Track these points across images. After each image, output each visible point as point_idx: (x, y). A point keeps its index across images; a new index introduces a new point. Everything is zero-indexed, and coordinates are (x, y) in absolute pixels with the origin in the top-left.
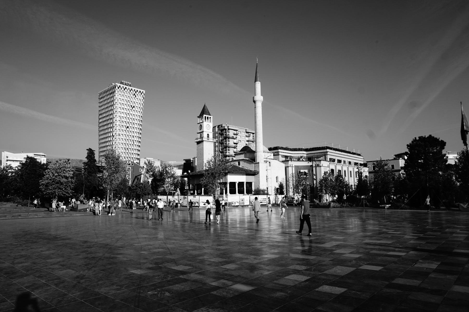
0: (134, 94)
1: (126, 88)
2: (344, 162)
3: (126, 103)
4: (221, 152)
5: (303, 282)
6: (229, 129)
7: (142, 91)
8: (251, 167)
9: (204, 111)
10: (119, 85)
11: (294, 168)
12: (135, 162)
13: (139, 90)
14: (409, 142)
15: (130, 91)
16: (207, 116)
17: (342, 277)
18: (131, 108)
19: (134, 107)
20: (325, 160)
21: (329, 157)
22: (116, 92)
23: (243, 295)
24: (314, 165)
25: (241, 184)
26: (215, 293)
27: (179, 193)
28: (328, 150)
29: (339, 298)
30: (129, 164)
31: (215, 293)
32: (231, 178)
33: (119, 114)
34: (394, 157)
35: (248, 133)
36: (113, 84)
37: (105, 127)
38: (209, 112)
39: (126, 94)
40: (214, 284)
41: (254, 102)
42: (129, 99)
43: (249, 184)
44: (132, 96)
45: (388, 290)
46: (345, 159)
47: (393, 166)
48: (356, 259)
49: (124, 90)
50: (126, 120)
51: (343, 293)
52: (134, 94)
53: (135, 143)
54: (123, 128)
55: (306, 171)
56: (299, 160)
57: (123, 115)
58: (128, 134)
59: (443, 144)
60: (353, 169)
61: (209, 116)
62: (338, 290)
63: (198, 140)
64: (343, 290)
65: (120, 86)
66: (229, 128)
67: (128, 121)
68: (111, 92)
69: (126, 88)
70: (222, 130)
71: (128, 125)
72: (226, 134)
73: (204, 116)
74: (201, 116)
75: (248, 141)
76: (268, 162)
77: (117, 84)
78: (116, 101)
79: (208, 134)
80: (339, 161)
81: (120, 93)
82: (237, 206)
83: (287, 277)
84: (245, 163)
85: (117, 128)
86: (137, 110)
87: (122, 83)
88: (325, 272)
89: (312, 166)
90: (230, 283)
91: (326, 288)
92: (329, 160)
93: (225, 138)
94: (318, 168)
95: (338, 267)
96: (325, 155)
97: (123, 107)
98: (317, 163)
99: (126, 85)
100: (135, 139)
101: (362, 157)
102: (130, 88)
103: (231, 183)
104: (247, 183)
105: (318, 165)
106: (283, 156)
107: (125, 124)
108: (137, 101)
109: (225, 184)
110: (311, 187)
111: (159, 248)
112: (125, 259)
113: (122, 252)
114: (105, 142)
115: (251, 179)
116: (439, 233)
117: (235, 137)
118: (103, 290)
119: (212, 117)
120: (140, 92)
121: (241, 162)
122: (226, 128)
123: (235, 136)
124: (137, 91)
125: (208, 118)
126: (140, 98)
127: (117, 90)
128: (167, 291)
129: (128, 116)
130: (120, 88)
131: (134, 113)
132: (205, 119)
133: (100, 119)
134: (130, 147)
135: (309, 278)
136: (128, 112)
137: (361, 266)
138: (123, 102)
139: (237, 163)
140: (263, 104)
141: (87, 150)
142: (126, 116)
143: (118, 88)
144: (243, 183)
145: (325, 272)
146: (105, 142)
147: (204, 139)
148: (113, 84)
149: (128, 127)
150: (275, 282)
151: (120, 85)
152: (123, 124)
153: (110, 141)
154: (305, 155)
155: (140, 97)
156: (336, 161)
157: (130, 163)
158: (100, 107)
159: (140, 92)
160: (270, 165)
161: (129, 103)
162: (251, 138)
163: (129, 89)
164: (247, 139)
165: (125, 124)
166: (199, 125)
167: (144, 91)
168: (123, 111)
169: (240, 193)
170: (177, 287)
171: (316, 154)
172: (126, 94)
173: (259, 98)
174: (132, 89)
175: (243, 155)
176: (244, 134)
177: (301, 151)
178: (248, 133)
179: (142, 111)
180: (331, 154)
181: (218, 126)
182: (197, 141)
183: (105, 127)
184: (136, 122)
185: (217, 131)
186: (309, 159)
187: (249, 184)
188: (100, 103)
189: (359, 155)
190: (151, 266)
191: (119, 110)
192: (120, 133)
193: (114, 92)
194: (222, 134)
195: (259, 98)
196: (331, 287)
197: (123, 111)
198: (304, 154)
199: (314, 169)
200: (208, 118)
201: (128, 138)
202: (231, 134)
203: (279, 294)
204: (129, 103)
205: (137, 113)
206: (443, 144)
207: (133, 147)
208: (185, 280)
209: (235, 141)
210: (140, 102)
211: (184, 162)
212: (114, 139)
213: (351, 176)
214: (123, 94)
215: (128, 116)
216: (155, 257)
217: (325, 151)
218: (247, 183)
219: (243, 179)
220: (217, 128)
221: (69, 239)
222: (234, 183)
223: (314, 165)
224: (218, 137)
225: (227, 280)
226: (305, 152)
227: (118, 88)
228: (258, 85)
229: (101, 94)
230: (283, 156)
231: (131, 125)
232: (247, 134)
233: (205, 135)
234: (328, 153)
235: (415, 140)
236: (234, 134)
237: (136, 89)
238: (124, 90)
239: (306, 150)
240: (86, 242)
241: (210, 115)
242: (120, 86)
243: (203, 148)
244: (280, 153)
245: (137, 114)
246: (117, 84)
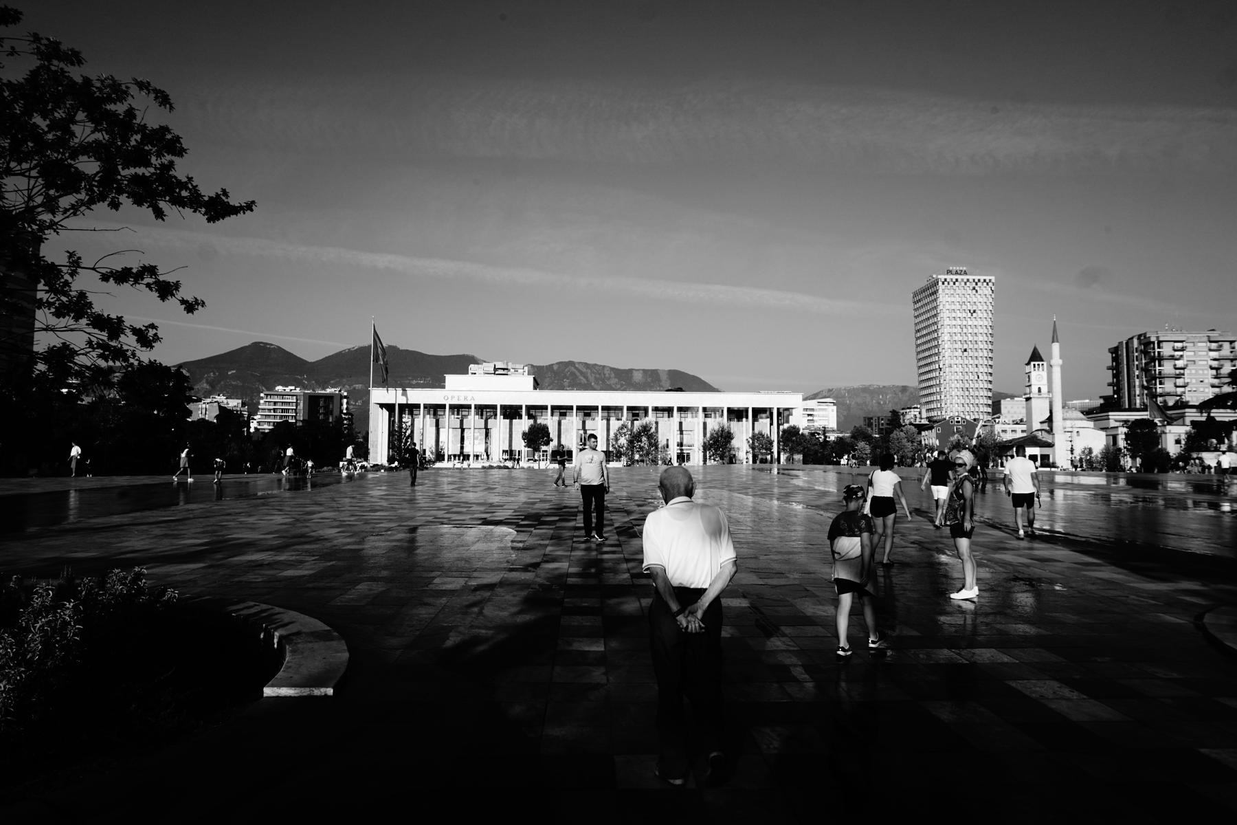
10: (942, 277)
13: (982, 278)
26: (1175, 675)
33: (946, 330)
37: (927, 354)
68: (929, 292)
85: (947, 355)
87: (949, 272)
93: (1153, 360)
99: (957, 273)
102: (965, 277)
122: (1153, 339)
123: (1178, 354)
133: (917, 339)
155: (985, 290)
164: (1214, 354)
167: (993, 278)
176: (1204, 345)
183: (927, 354)
193: (936, 292)
194: (1145, 353)
202: (1167, 350)
205: (982, 322)
209: (1180, 363)
211: (1102, 401)
229: (915, 295)
232: (1214, 346)
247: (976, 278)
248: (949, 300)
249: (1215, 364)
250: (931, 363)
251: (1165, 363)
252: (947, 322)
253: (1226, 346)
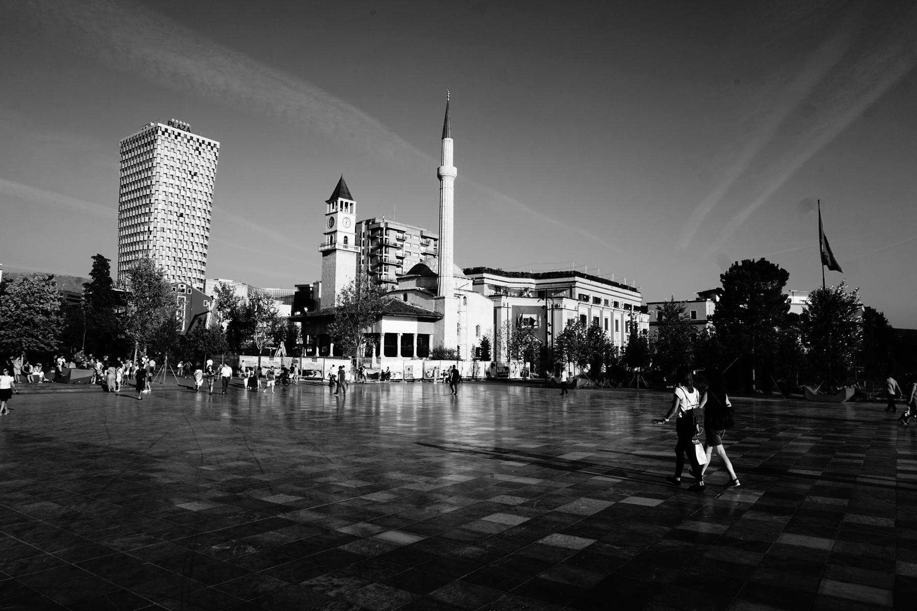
0: (197, 149)
1: (179, 134)
2: (606, 302)
3: (179, 165)
4: (371, 274)
5: (515, 527)
6: (387, 229)
7: (213, 142)
8: (428, 305)
9: (340, 191)
10: (164, 127)
11: (510, 310)
12: (195, 286)
13: (207, 140)
14: (725, 270)
15: (189, 141)
16: (345, 201)
17: (589, 519)
18: (190, 177)
19: (195, 174)
20: (571, 297)
21: (577, 292)
22: (159, 142)
23: (401, 550)
24: (549, 306)
25: (407, 338)
26: (346, 547)
27: (284, 353)
28: (577, 278)
29: (580, 558)
30: (183, 291)
31: (346, 547)
32: (388, 326)
33: (163, 188)
34: (698, 296)
35: (425, 237)
36: (152, 124)
37: (134, 213)
38: (349, 194)
39: (179, 148)
40: (345, 530)
41: (440, 177)
42: (186, 159)
43: (424, 338)
44: (192, 152)
45: (669, 543)
46: (607, 297)
47: (694, 313)
48: (615, 485)
49: (176, 138)
50: (177, 201)
51: (588, 548)
52: (197, 149)
53: (196, 249)
54: (170, 217)
55: (534, 317)
56: (521, 294)
57: (171, 190)
58: (181, 228)
59: (783, 276)
60: (622, 316)
61: (350, 202)
62: (579, 543)
63: (326, 248)
64: (588, 542)
65: (166, 130)
67: (183, 202)
68: (148, 140)
69: (179, 134)
70: (374, 231)
71: (182, 211)
72: (382, 239)
73: (340, 199)
74: (333, 200)
75: (424, 254)
76: (462, 297)
77: (159, 124)
78: (158, 160)
79: (346, 237)
80: (597, 301)
81: (167, 144)
82: (398, 381)
83: (486, 519)
84: (418, 297)
85: (159, 216)
86: (202, 180)
87: (170, 123)
88: (557, 509)
89: (545, 308)
90: (376, 529)
91: (558, 539)
92: (577, 297)
93: (380, 246)
94: (556, 312)
95: (583, 499)
96: (571, 287)
97: (172, 172)
98: (556, 302)
99: (179, 127)
100: (197, 240)
101: (639, 295)
102: (189, 135)
103: (387, 335)
104: (419, 335)
105: (557, 306)
106: (492, 286)
107: (176, 209)
108: (203, 164)
109: (377, 336)
110: (541, 349)
111: (238, 460)
112: (168, 481)
113: (161, 466)
114: (132, 244)
115: (427, 328)
116: (767, 440)
117: (398, 246)
118: (118, 543)
119: (354, 203)
120: (209, 144)
121: (409, 295)
122: (382, 225)
124: (203, 142)
125: (346, 204)
126: (210, 157)
127: (160, 138)
128: (250, 544)
129: (183, 193)
130: (167, 134)
131: (195, 187)
132: (341, 206)
133: (122, 195)
134: (185, 256)
135: (527, 519)
136: (184, 184)
137: (624, 497)
138: (172, 164)
139: (402, 297)
140: (457, 183)
141: (94, 257)
142: (177, 192)
143: (163, 133)
144: (411, 335)
145: (557, 509)
146: (132, 244)
147: (337, 247)
148: (152, 124)
149: (181, 215)
150: (463, 526)
152: (171, 208)
153: (143, 242)
154: (534, 287)
155: (209, 155)
156: (591, 300)
157: (185, 287)
158: (123, 170)
159: (209, 144)
160: (465, 303)
161: (185, 167)
162: (431, 249)
163: (186, 136)
164: (423, 249)
165: (176, 209)
166: (329, 217)
167: (218, 144)
168: (171, 181)
169: (404, 354)
170: (271, 536)
171: (554, 285)
172: (179, 148)
173: (449, 170)
174: (192, 138)
175: (414, 281)
177: (527, 277)
178: (425, 237)
179: (212, 183)
180: (582, 286)
181: (367, 222)
182: (323, 249)
183: (134, 213)
184: (199, 205)
185: (363, 231)
186: (541, 294)
187: (424, 338)
188: (123, 162)
189: (634, 290)
190: (220, 495)
191: (163, 179)
192: (165, 226)
193: (153, 142)
194: (373, 239)
195: (449, 170)
196: (567, 537)
197: (171, 181)
198: (532, 284)
199: (549, 313)
200: (346, 204)
201: (181, 237)
202: (392, 237)
203: (469, 550)
204: (185, 167)
205: (202, 188)
206: (783, 276)
207: (191, 257)
208: (289, 523)
209: (400, 253)
210: (208, 165)
211: (296, 290)
212: (151, 238)
213: (617, 330)
214: (173, 146)
215: (183, 193)
216: (230, 477)
217: (571, 279)
218: (419, 335)
220: (364, 226)
221: (49, 439)
222: (395, 335)
223: (549, 306)
224: (366, 243)
225: (371, 522)
226: (533, 281)
228: (449, 144)
229: (125, 144)
230: (492, 286)
231: (188, 212)
232: (424, 241)
233: (340, 238)
234: (577, 284)
235: (735, 267)
236: (398, 239)
237: (201, 139)
238: (176, 138)
239: (536, 276)
240: (85, 446)
241: (351, 199)
242: (166, 130)
243: (334, 264)
244: (486, 281)
245: (201, 189)
246: (159, 124)
247: (201, 139)
250: (137, 225)
252: (163, 179)
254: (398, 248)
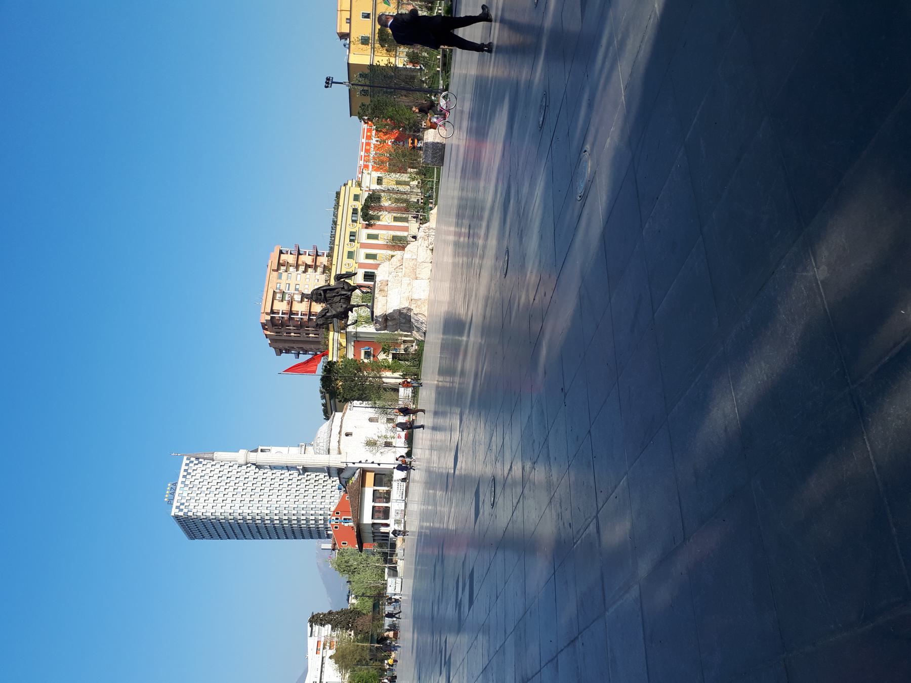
13: (184, 467)
25: (376, 496)
65: (177, 507)
66: (269, 311)
82: (406, 504)
87: (170, 502)
99: (173, 494)
101: (343, 188)
102: (179, 485)
122: (268, 318)
124: (186, 470)
130: (182, 507)
151: (174, 507)
169: (388, 500)
189: (338, 194)
209: (298, 297)
219: (369, 491)
222: (374, 507)
227: (182, 510)
237: (182, 473)
248: (204, 506)
249: (302, 268)
251: (294, 309)
252: (227, 509)
253: (284, 257)
254: (292, 298)
